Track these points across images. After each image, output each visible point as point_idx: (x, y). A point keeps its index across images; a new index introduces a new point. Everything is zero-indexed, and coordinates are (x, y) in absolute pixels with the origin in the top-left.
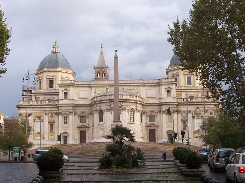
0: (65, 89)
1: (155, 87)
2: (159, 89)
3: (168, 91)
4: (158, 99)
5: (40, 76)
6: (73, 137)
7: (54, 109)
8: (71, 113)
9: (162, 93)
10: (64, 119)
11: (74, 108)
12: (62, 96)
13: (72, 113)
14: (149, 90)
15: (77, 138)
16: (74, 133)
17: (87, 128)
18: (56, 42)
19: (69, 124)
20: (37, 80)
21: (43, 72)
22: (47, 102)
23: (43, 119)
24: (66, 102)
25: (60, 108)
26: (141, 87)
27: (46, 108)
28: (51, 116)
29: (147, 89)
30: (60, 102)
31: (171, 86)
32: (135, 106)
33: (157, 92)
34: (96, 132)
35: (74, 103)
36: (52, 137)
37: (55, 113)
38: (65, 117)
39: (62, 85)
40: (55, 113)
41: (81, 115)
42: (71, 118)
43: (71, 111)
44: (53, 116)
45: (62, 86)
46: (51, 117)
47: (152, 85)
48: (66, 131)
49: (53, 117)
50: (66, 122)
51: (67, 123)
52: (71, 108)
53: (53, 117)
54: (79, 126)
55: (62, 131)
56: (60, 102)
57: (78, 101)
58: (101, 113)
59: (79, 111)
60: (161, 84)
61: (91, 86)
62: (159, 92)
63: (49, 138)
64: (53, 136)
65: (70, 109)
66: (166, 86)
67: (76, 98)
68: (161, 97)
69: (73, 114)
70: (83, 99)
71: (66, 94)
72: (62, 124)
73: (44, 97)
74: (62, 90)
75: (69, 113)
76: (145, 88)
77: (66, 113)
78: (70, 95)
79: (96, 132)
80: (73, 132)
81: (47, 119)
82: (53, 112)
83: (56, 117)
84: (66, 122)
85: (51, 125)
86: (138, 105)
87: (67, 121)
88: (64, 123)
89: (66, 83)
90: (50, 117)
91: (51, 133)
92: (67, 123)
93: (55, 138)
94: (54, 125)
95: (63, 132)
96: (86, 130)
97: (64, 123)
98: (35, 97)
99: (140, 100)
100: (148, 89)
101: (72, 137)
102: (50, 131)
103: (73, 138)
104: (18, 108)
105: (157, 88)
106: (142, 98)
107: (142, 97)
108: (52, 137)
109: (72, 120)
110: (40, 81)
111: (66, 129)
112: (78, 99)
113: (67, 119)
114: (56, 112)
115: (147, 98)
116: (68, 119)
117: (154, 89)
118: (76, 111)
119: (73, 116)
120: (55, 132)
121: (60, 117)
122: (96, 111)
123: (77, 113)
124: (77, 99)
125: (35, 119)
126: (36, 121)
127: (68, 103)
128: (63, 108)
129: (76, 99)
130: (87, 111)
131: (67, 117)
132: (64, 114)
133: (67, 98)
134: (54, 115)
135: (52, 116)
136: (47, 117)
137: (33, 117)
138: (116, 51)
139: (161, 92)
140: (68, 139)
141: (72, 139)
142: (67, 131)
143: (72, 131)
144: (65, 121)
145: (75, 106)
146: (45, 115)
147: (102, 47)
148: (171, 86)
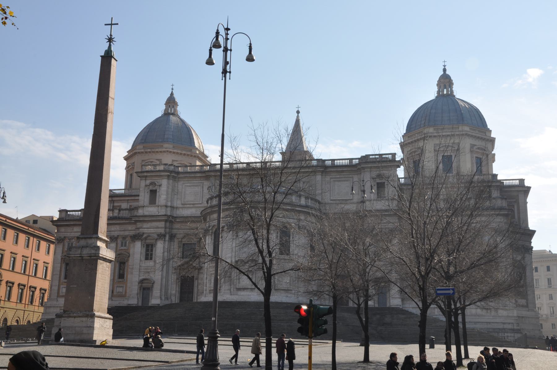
0: (151, 184)
1: (351, 176)
3: (381, 186)
4: (358, 203)
5: (132, 161)
6: (163, 291)
7: (130, 227)
8: (161, 236)
10: (147, 250)
11: (168, 224)
12: (144, 198)
13: (164, 236)
14: (337, 183)
15: (174, 292)
16: (167, 281)
17: (197, 271)
18: (172, 94)
19: (155, 261)
21: (136, 153)
24: (152, 210)
25: (139, 225)
26: (319, 177)
27: (113, 226)
28: (122, 243)
29: (332, 180)
30: (140, 212)
31: (385, 172)
32: (295, 217)
34: (207, 278)
35: (169, 214)
36: (120, 290)
38: (148, 246)
39: (145, 174)
40: (131, 237)
41: (185, 241)
42: (160, 248)
43: (162, 231)
45: (146, 176)
46: (122, 246)
47: (343, 171)
48: (148, 277)
49: (125, 246)
50: (149, 256)
51: (151, 259)
52: (162, 224)
53: (125, 246)
54: (179, 264)
55: (139, 276)
56: (140, 212)
57: (181, 210)
59: (181, 231)
60: (364, 168)
61: (210, 176)
63: (115, 293)
64: (123, 287)
66: (375, 173)
67: (177, 203)
69: (167, 238)
70: (192, 206)
71: (153, 193)
72: (141, 260)
74: (146, 186)
75: (158, 235)
76: (328, 178)
77: (149, 236)
78: (162, 196)
79: (207, 278)
80: (164, 280)
82: (127, 233)
84: (149, 256)
86: (302, 217)
87: (152, 255)
88: (147, 259)
89: (155, 170)
90: (119, 245)
91: (121, 280)
92: (151, 259)
93: (126, 292)
94: (126, 264)
95: (142, 278)
96: (195, 273)
97: (147, 259)
99: (310, 204)
100: (335, 181)
101: (161, 290)
102: (116, 277)
103: (163, 293)
104: (56, 225)
105: (356, 178)
106: (316, 201)
107: (320, 200)
108: (120, 290)
109: (163, 253)
110: (131, 173)
111: (149, 272)
112: (181, 206)
113: (152, 250)
114: (132, 233)
115: (332, 202)
117: (347, 181)
118: (174, 231)
119: (167, 243)
120: (127, 276)
123: (178, 236)
124: (178, 206)
127: (157, 214)
128: (145, 225)
129: (175, 205)
132: (146, 238)
133: (155, 204)
134: (128, 240)
138: (110, 40)
140: (151, 294)
141: (159, 294)
142: (152, 275)
143: (160, 277)
145: (170, 220)
147: (298, 112)
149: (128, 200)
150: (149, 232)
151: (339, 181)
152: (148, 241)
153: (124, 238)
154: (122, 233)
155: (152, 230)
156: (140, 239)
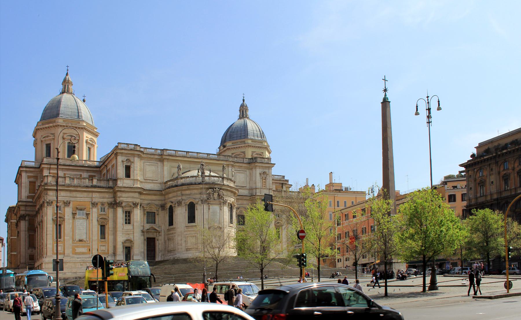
2: (250, 174)
9: (255, 181)
10: (126, 216)
13: (138, 204)
20: (42, 141)
22: (76, 182)
23: (87, 215)
28: (102, 208)
31: (267, 171)
33: (248, 179)
37: (108, 204)
38: (126, 212)
42: (138, 215)
44: (104, 208)
46: (101, 211)
49: (104, 211)
53: (104, 211)
58: (192, 208)
62: (251, 179)
65: (136, 198)
68: (254, 186)
73: (65, 172)
77: (128, 204)
81: (95, 213)
82: (105, 200)
83: (111, 210)
85: (101, 226)
98: (48, 171)
105: (248, 172)
113: (129, 216)
116: (132, 215)
121: (120, 211)
122: (179, 203)
125: (74, 214)
126: (77, 216)
130: (157, 203)
131: (129, 212)
132: (125, 206)
135: (103, 210)
136: (95, 210)
137: (71, 210)
139: (254, 180)
144: (126, 220)
146: (91, 207)
148: (267, 171)
149: (63, 169)
150: (127, 201)
151: (239, 173)
152: (128, 209)
153: (103, 204)
154: (102, 200)
155: (130, 200)
156: (120, 206)
